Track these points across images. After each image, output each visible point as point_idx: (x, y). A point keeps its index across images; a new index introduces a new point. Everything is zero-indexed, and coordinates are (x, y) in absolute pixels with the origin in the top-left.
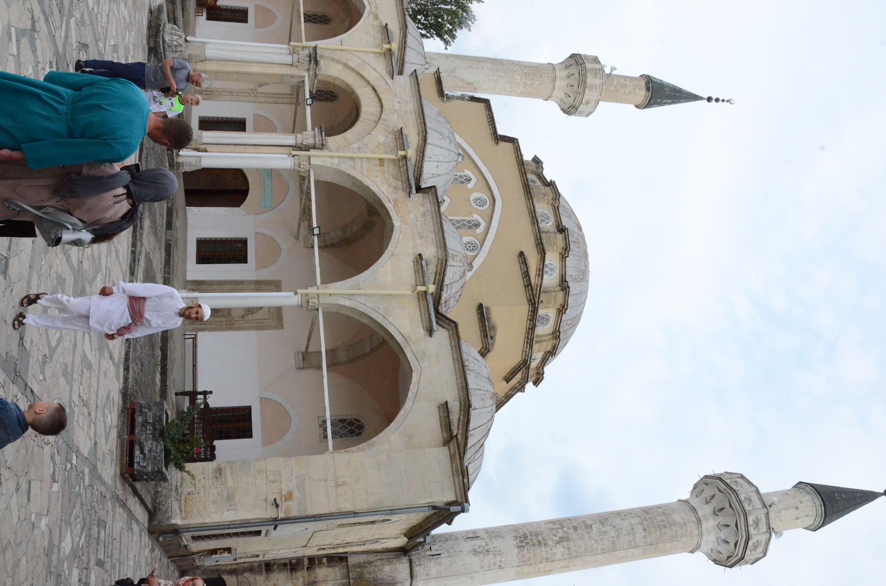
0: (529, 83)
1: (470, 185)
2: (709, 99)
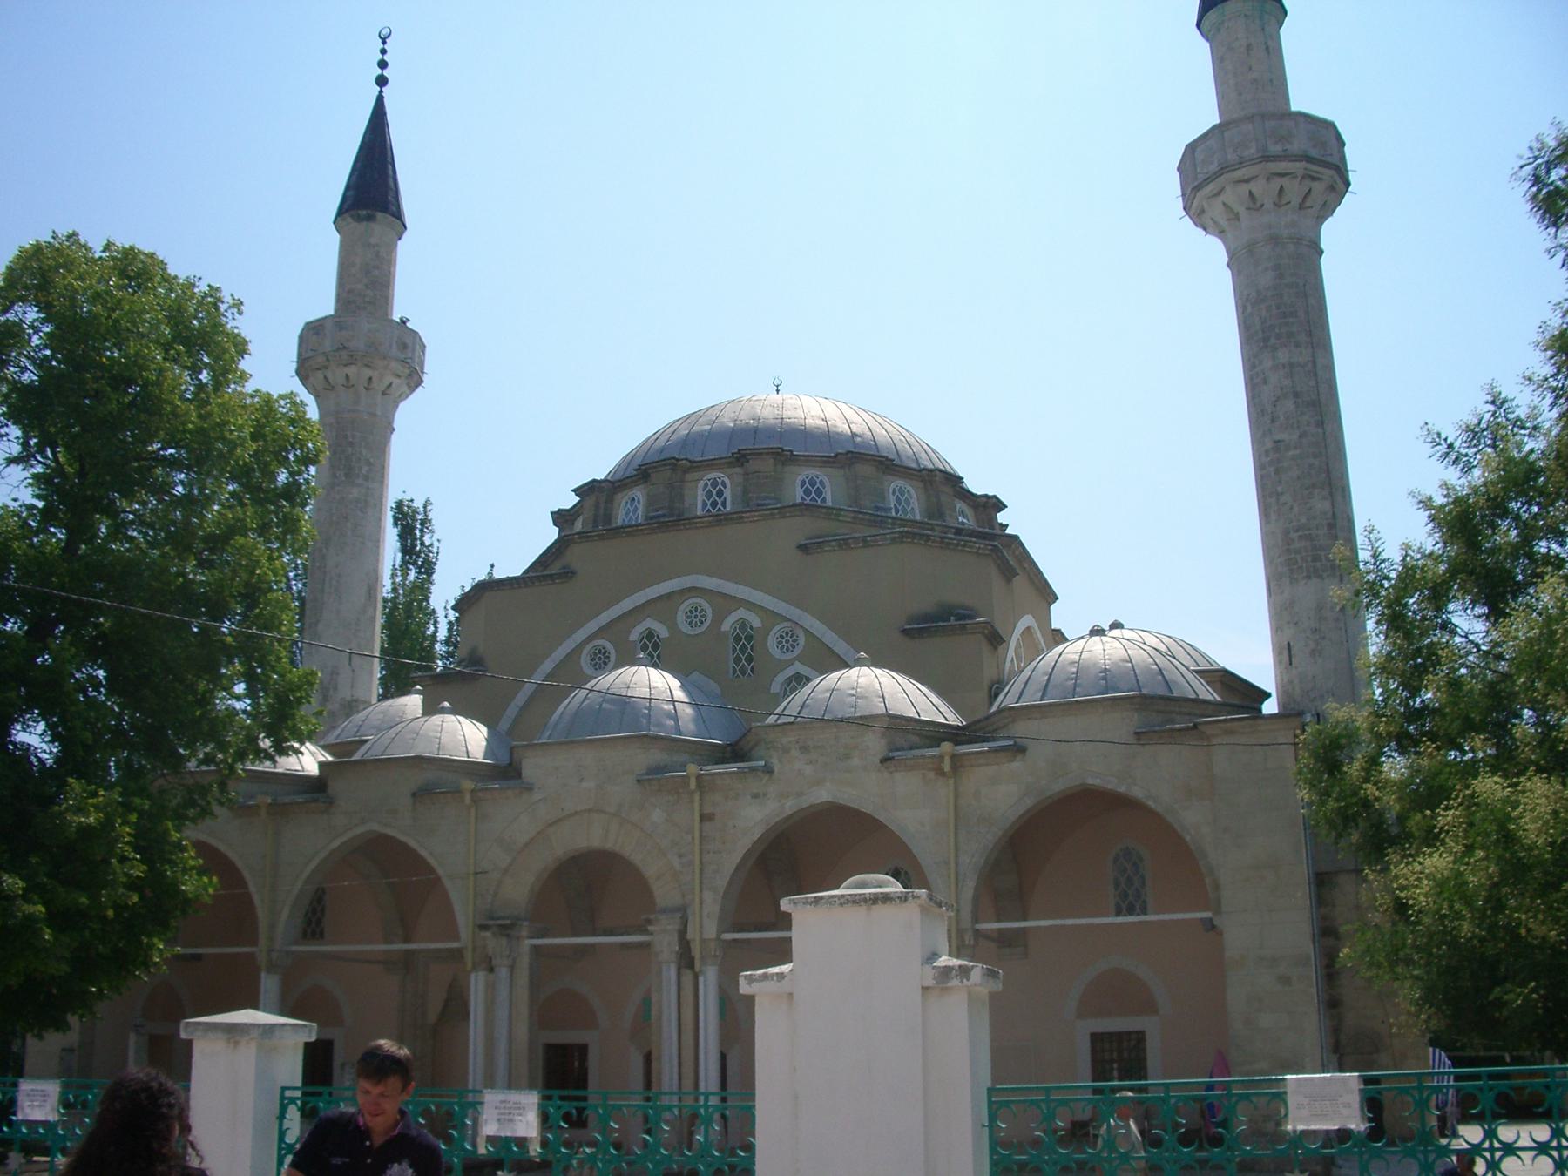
0: (365, 469)
1: (662, 631)
2: (382, 81)
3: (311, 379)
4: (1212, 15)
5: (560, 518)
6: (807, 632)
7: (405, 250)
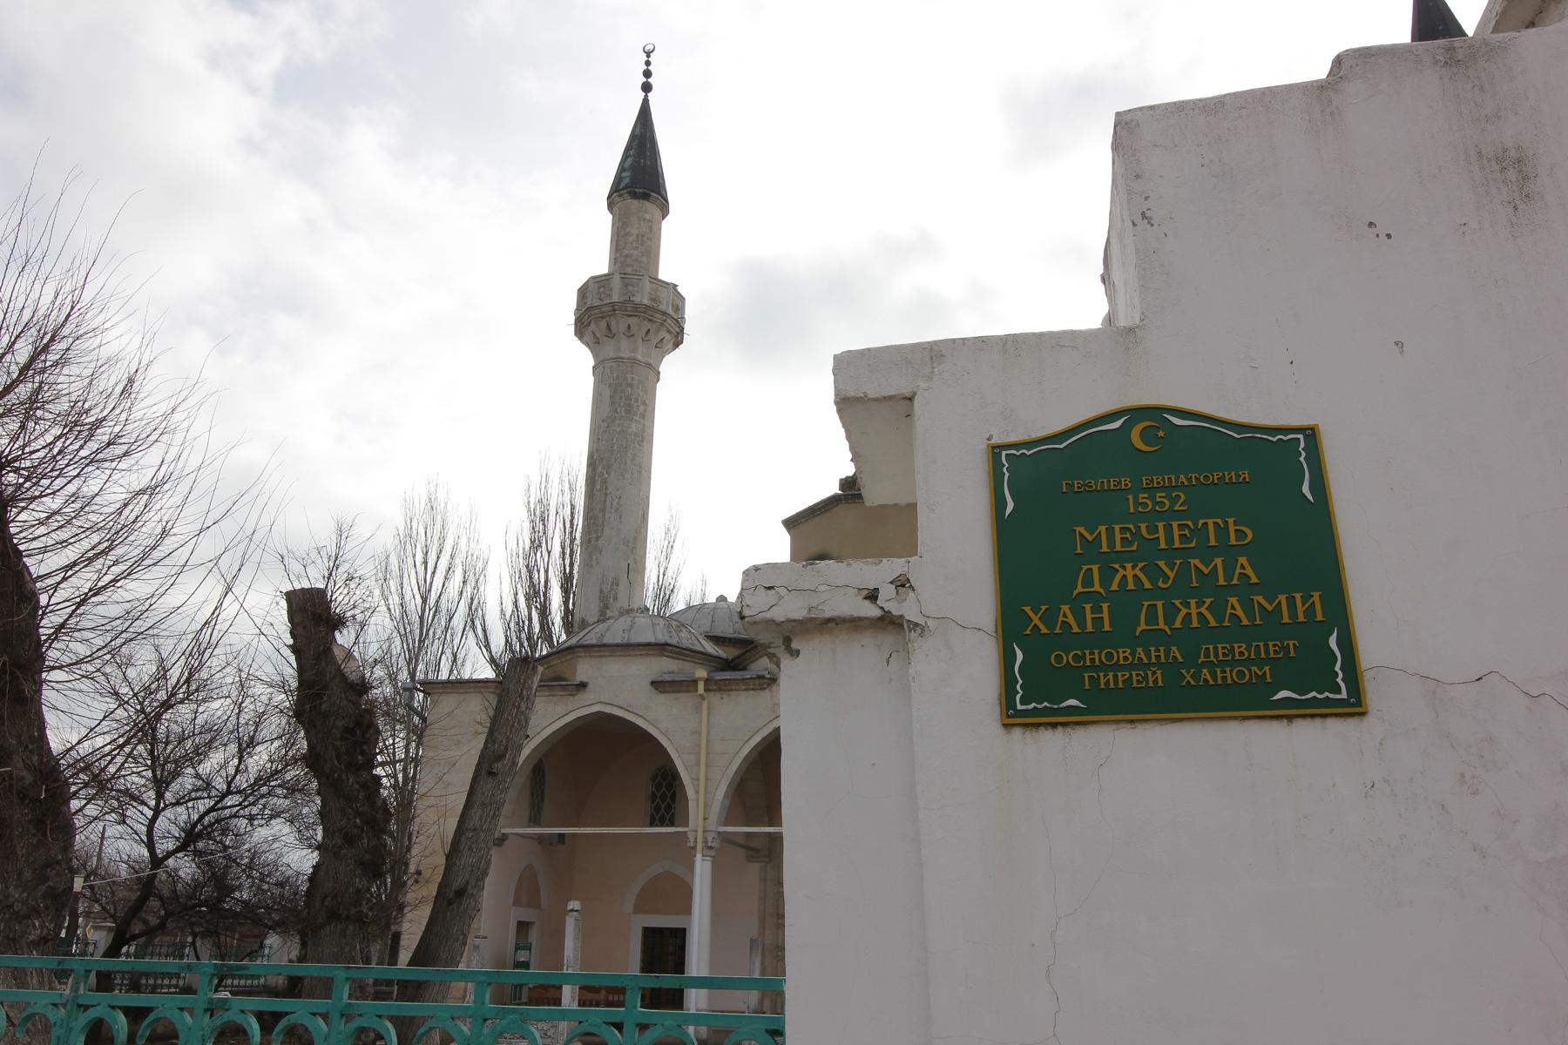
2: (647, 88)
3: (593, 326)
7: (668, 227)
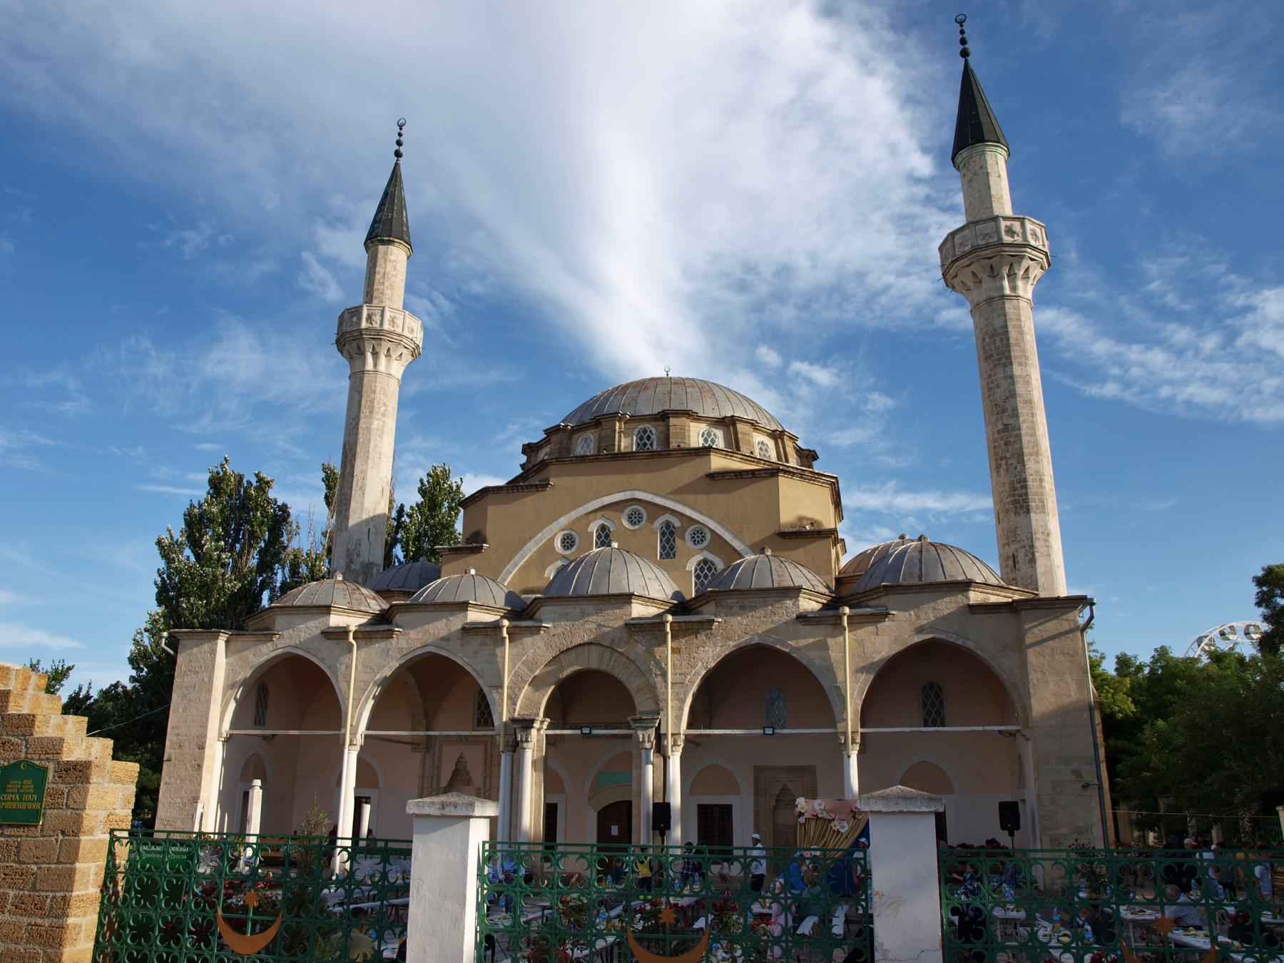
0: (383, 409)
2: (398, 154)
4: (964, 153)
5: (528, 449)
6: (713, 532)
